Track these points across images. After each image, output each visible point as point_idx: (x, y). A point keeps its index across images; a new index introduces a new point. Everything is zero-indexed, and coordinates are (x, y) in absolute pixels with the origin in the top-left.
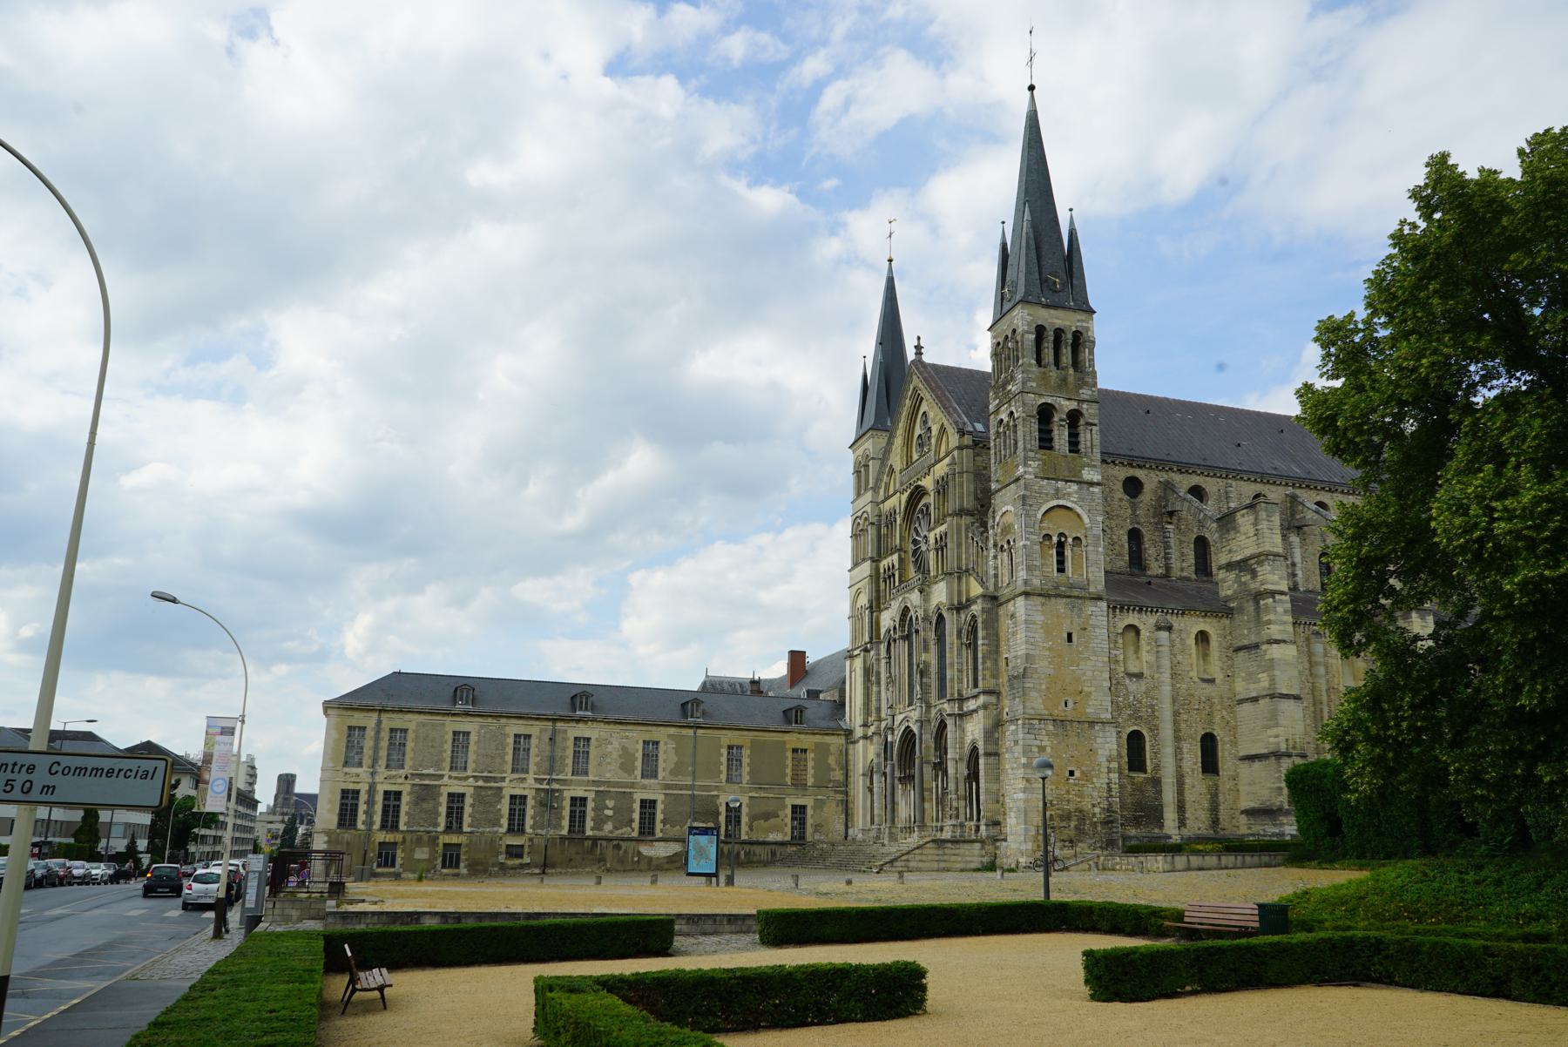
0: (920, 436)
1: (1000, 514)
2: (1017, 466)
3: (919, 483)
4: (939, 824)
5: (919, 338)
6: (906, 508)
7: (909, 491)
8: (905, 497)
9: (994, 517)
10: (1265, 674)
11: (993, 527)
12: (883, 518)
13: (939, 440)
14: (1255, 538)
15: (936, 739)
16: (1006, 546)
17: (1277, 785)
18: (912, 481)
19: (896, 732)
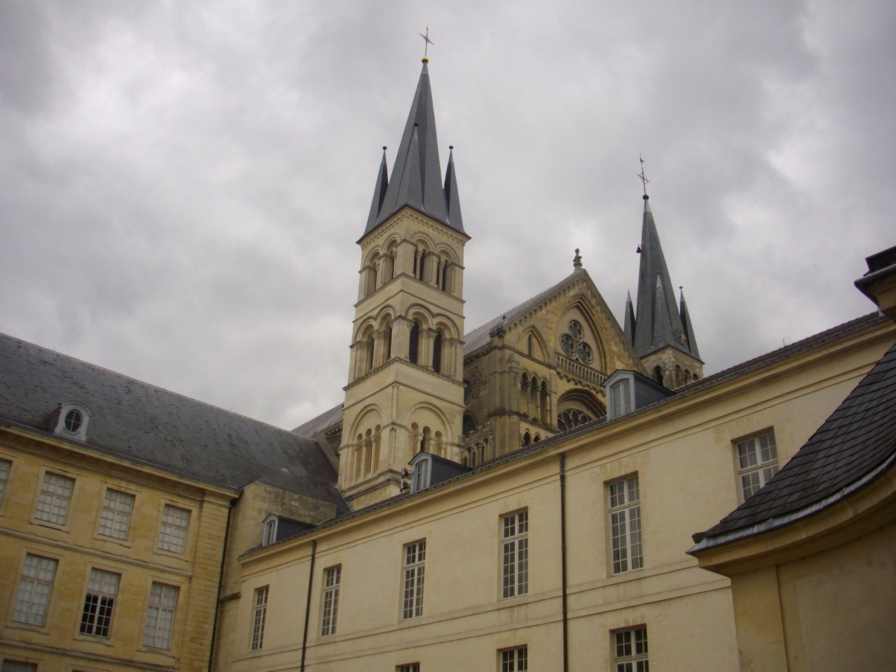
0: (567, 337)
3: (593, 392)
5: (577, 251)
7: (571, 386)
18: (584, 382)
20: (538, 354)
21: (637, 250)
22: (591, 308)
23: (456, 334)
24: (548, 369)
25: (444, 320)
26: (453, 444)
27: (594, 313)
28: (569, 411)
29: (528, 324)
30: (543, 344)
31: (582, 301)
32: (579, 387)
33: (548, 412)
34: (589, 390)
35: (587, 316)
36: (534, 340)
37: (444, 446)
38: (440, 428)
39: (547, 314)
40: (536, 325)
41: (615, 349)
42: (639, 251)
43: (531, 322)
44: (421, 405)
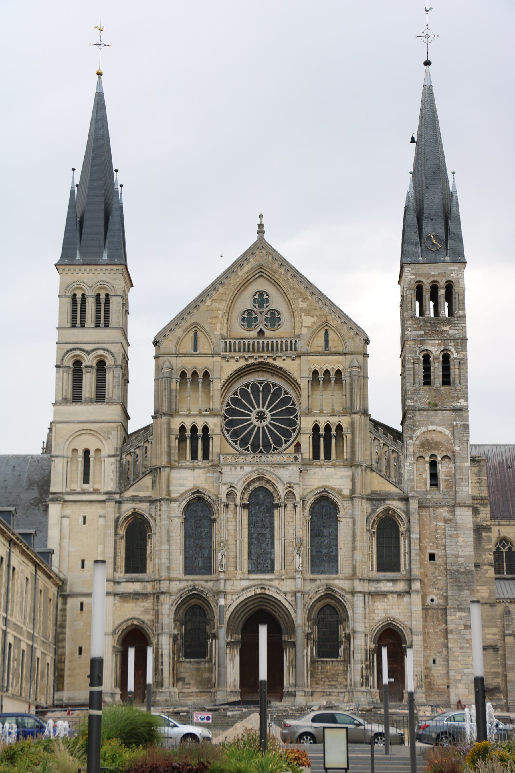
0: (250, 312)
1: (423, 429)
2: (458, 398)
3: (270, 361)
4: (310, 690)
5: (261, 216)
6: (231, 376)
7: (242, 363)
8: (232, 367)
9: (414, 431)
10: (484, 588)
11: (411, 438)
12: (177, 376)
13: (314, 334)
14: (478, 485)
15: (309, 610)
16: (427, 459)
17: (493, 670)
18: (256, 356)
19: (229, 597)
20: (204, 347)
21: (410, 140)
22: (273, 274)
23: (113, 360)
24: (211, 358)
25: (101, 352)
26: (109, 456)
27: (278, 277)
28: (247, 386)
29: (188, 324)
30: (207, 334)
31: (263, 270)
32: (251, 361)
33: (211, 398)
34: (263, 361)
35: (273, 281)
36: (199, 334)
37: (103, 459)
38: (99, 446)
39: (211, 304)
40: (198, 321)
41: (303, 305)
42: (413, 141)
43: (191, 320)
44: (76, 435)
